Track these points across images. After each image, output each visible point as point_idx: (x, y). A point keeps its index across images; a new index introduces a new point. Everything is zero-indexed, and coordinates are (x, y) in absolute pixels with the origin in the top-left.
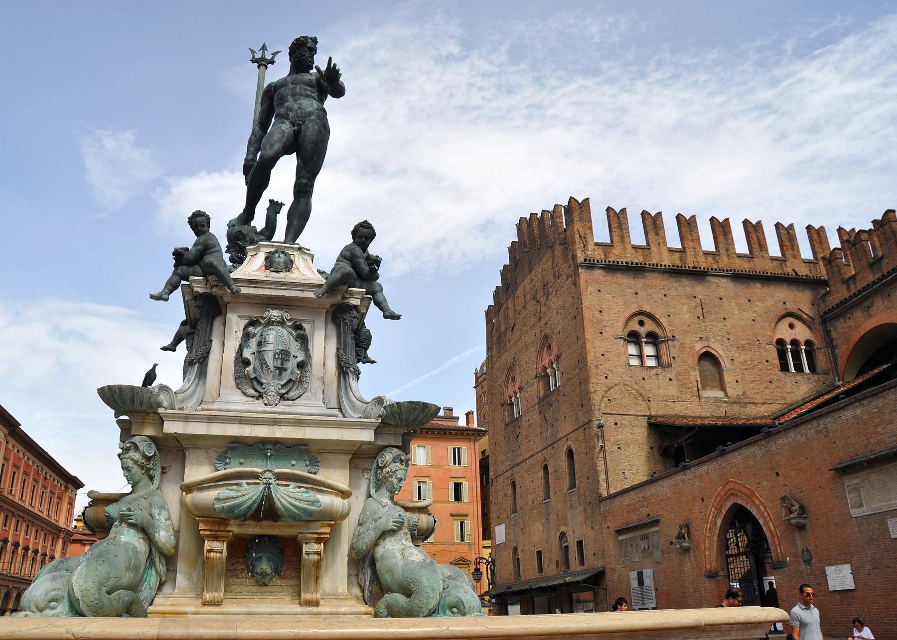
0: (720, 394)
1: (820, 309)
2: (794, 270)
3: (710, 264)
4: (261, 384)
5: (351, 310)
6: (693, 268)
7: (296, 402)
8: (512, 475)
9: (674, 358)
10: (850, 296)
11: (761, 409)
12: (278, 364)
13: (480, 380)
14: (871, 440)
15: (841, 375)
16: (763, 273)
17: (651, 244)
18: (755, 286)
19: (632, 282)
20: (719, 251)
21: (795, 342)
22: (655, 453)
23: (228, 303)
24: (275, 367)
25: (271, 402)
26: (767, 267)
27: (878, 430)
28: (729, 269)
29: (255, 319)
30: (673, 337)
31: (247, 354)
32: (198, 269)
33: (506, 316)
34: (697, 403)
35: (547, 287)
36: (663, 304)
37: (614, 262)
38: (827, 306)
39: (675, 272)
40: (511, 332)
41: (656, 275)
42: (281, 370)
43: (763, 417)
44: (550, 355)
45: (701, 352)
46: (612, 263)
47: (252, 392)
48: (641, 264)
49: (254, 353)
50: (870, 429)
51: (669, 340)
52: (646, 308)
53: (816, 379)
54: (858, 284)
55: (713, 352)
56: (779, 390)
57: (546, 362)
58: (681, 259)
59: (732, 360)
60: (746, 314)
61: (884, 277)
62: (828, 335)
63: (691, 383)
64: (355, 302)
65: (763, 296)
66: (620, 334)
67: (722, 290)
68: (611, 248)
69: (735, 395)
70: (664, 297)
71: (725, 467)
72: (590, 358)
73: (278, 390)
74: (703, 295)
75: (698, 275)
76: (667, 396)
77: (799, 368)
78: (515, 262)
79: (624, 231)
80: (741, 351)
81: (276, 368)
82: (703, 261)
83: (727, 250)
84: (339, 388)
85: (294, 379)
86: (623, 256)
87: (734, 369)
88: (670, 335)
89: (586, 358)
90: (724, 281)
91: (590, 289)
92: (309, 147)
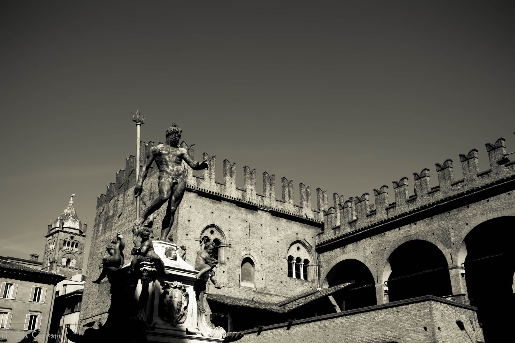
0: (251, 285)
1: (316, 241)
2: (306, 214)
3: (259, 202)
6: (248, 202)
8: (100, 319)
9: (228, 258)
10: (335, 238)
11: (273, 299)
12: (179, 307)
14: (348, 338)
15: (321, 284)
16: (288, 213)
17: (227, 182)
18: (282, 220)
19: (211, 205)
20: (265, 194)
21: (298, 260)
22: (208, 318)
24: (177, 309)
26: (291, 210)
27: (353, 333)
28: (269, 207)
30: (230, 244)
32: (146, 258)
33: (115, 206)
34: (237, 289)
35: (153, 195)
37: (202, 189)
38: (321, 241)
40: (117, 218)
41: (226, 203)
43: (274, 304)
45: (244, 257)
46: (201, 190)
48: (219, 194)
50: (349, 332)
51: (227, 246)
52: (217, 224)
53: (307, 284)
54: (341, 232)
55: (251, 258)
56: (285, 288)
58: (242, 195)
59: (262, 265)
60: (274, 237)
61: (356, 232)
62: (318, 258)
63: (236, 276)
65: (286, 227)
67: (263, 219)
68: (202, 180)
69: (260, 288)
70: (229, 218)
71: (261, 338)
76: (220, 282)
77: (298, 276)
78: (130, 170)
79: (212, 171)
80: (267, 260)
82: (255, 199)
84: (198, 319)
86: (208, 186)
87: (262, 271)
88: (228, 244)
90: (265, 214)
91: (185, 205)
92: (179, 192)
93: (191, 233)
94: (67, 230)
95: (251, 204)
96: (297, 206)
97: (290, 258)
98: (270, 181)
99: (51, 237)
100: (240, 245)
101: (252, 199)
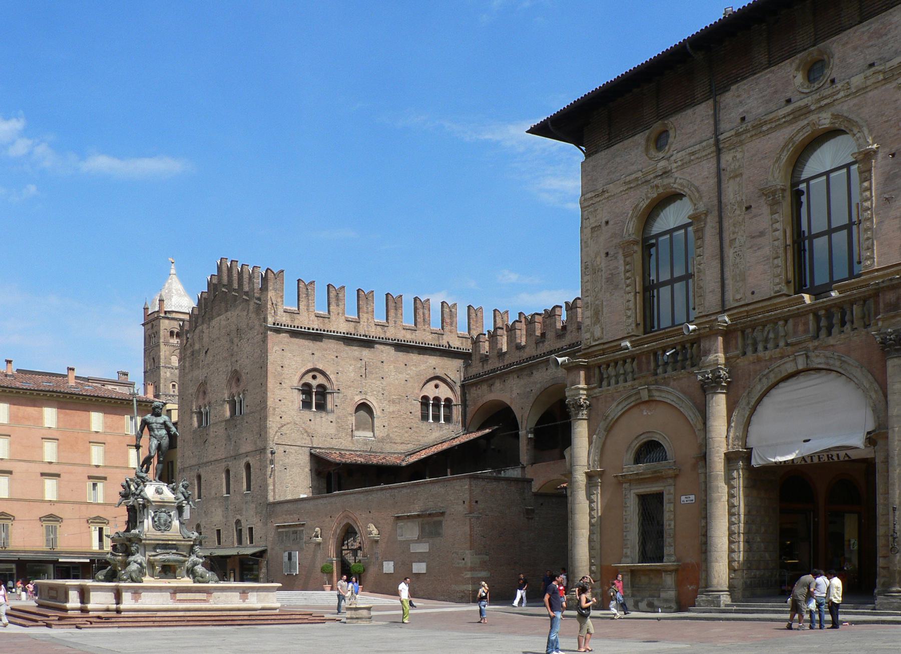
2: (448, 343)
13: (151, 318)
16: (422, 343)
30: (339, 390)
36: (334, 364)
39: (348, 340)
44: (238, 386)
52: (320, 366)
57: (234, 391)
60: (400, 376)
66: (296, 385)
67: (385, 355)
72: (270, 403)
74: (368, 358)
75: (367, 343)
82: (373, 330)
83: (395, 322)
88: (336, 388)
89: (267, 402)
93: (286, 381)
94: (174, 315)
95: (368, 338)
96: (434, 333)
97: (425, 401)
98: (394, 304)
99: (149, 326)
100: (352, 389)
101: (368, 331)
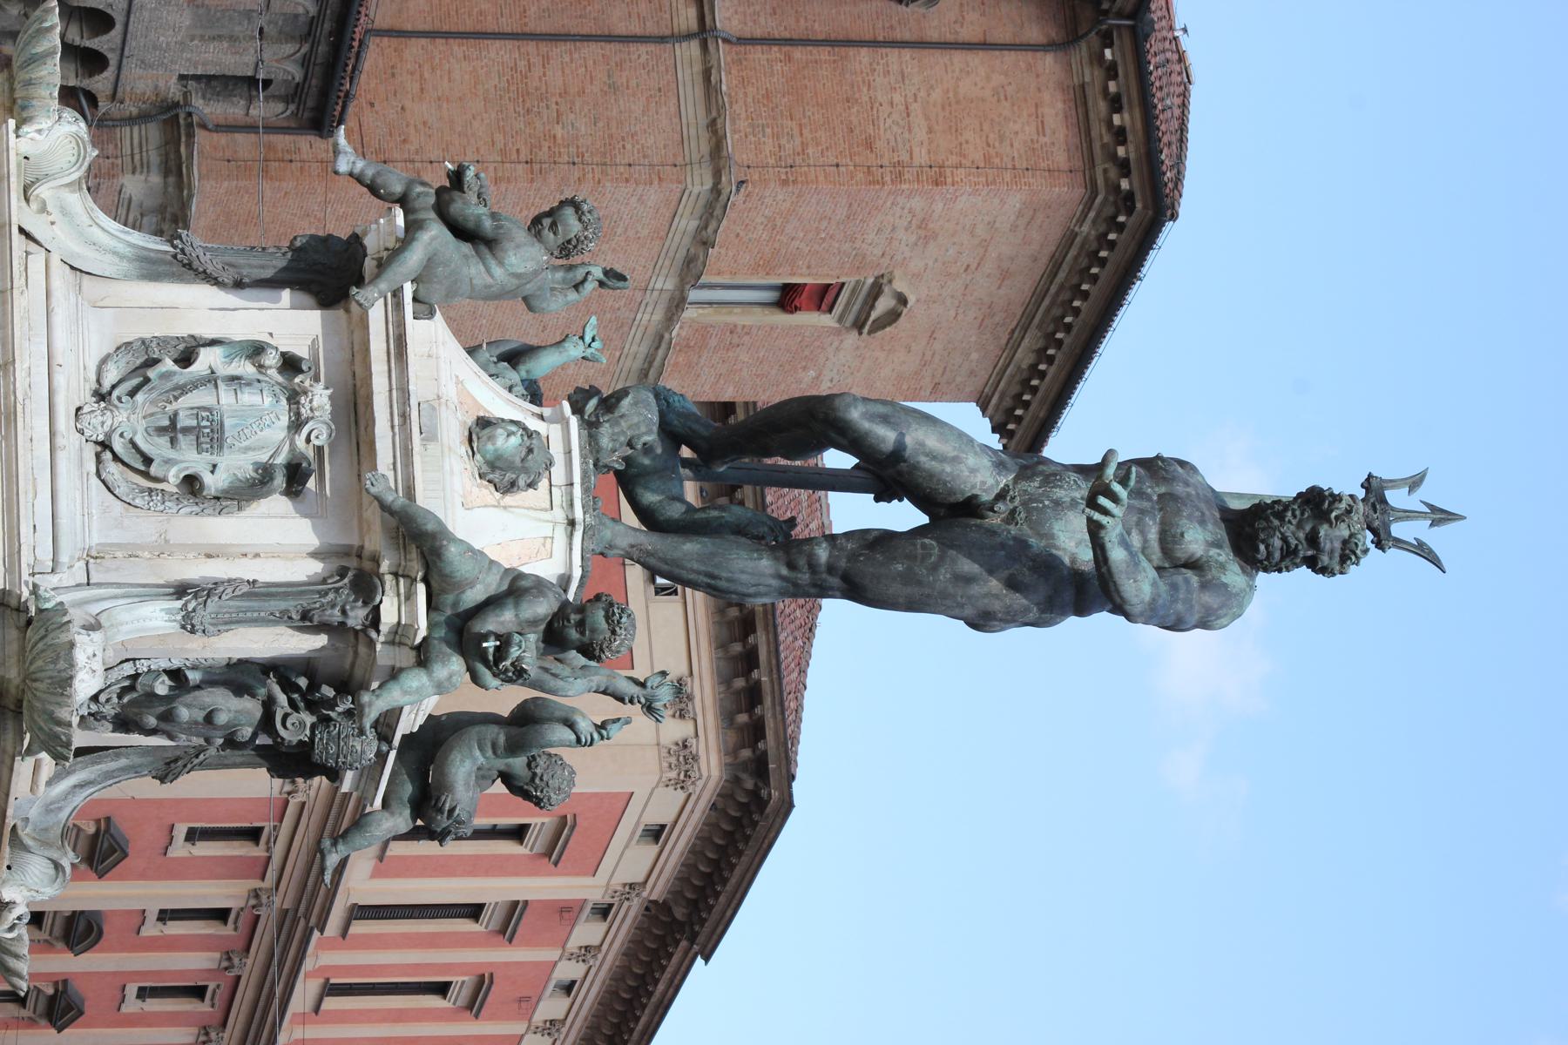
4: (132, 393)
5: (365, 603)
7: (95, 481)
12: (185, 421)
23: (347, 311)
24: (176, 414)
25: (85, 419)
29: (304, 368)
31: (207, 359)
42: (171, 430)
47: (110, 377)
49: (213, 372)
64: (389, 613)
73: (119, 431)
81: (174, 419)
85: (153, 470)
